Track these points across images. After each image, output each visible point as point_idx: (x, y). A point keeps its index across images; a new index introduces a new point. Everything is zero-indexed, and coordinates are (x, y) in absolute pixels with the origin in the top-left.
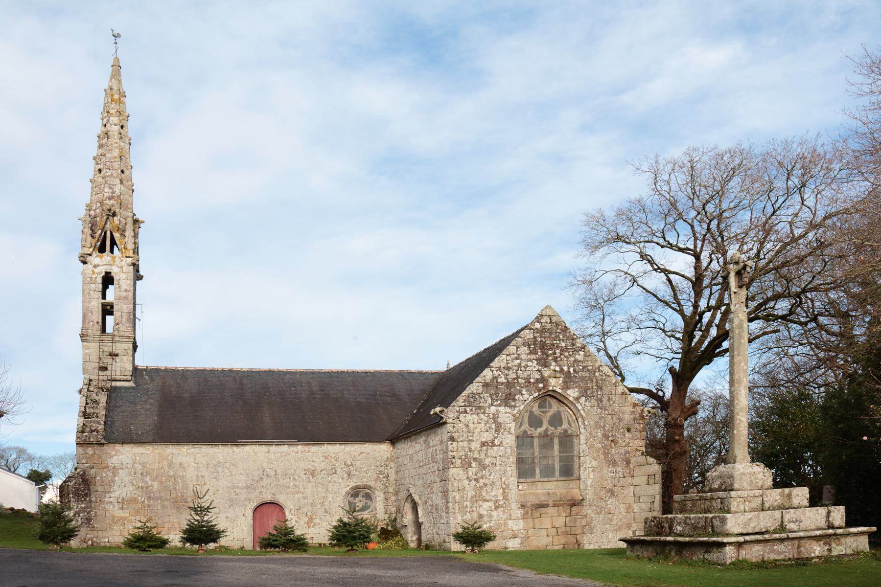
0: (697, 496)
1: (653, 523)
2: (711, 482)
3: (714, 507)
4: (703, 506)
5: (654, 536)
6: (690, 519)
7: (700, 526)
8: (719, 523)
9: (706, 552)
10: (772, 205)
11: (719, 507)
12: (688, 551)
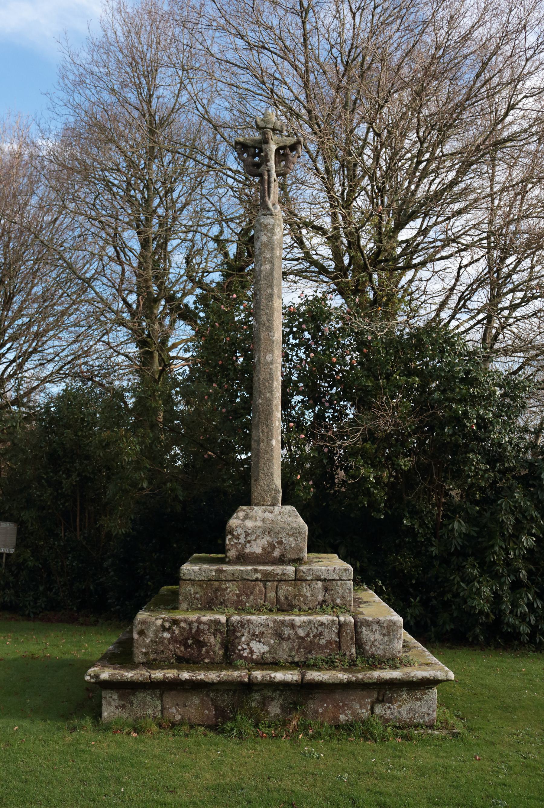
0: (256, 571)
1: (167, 635)
2: (242, 540)
3: (305, 597)
4: (273, 594)
5: (171, 666)
6: (292, 626)
7: (323, 642)
8: (378, 636)
9: (379, 701)
10: (460, 268)
11: (320, 598)
12: (325, 702)
